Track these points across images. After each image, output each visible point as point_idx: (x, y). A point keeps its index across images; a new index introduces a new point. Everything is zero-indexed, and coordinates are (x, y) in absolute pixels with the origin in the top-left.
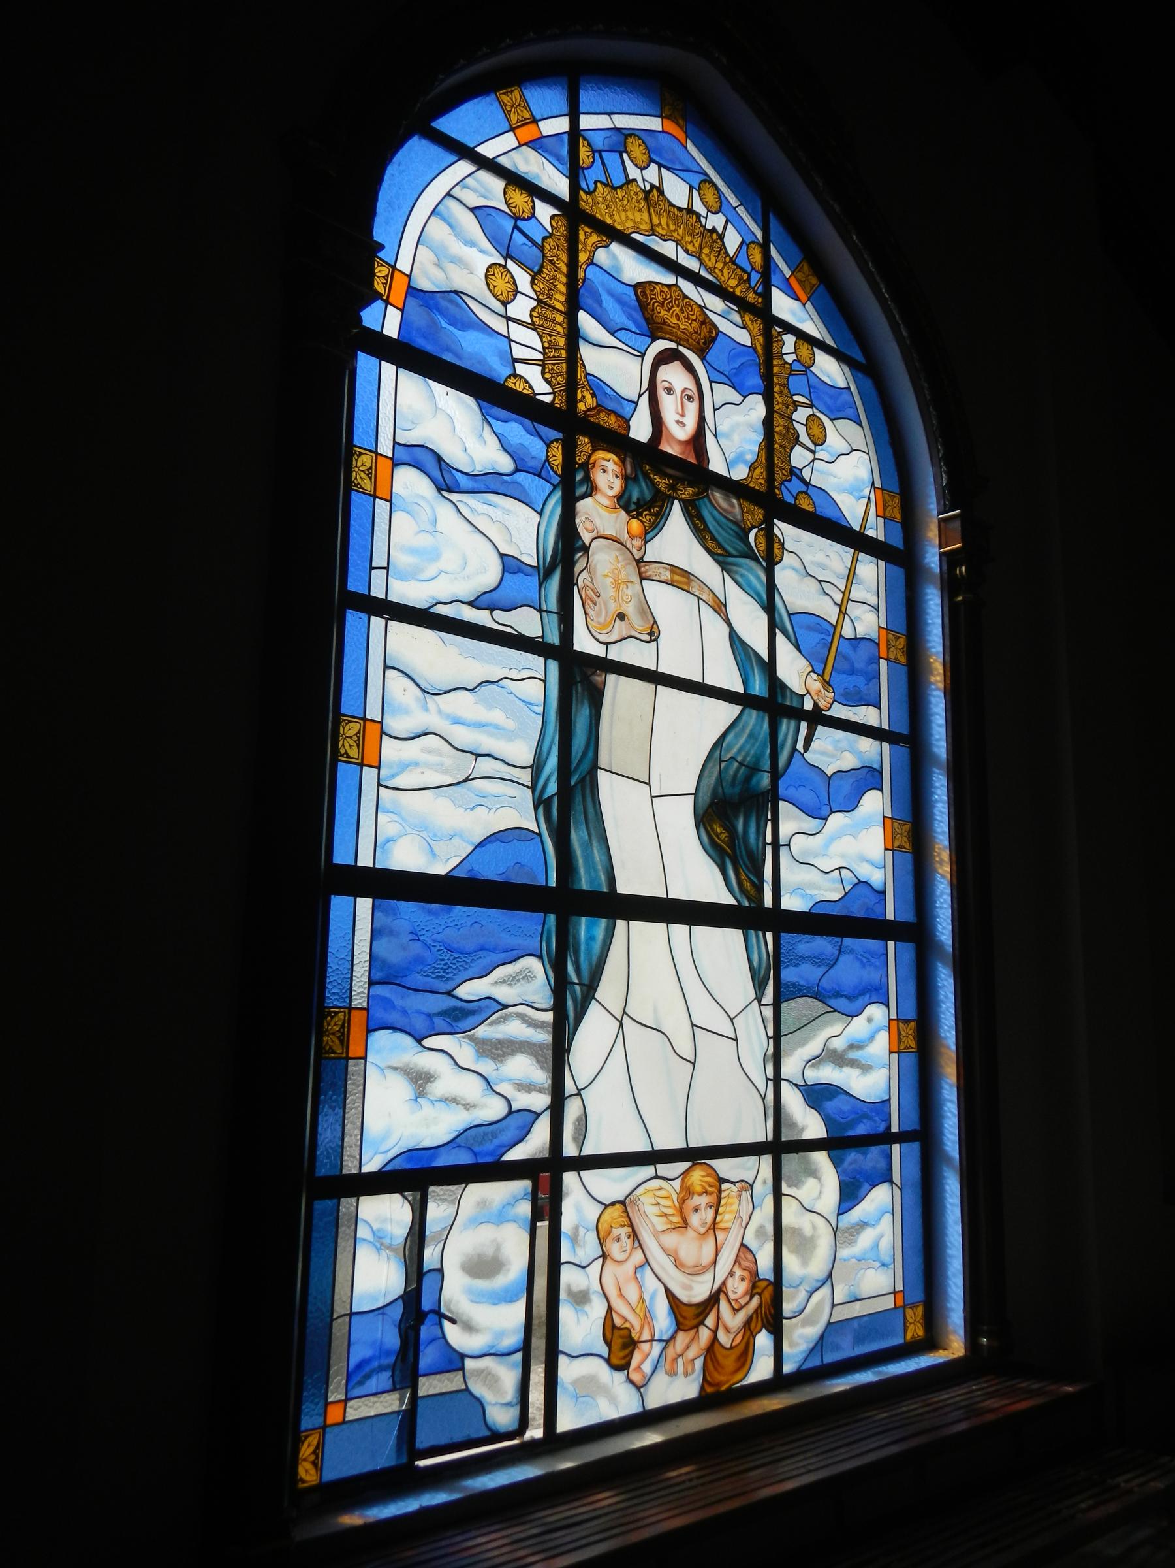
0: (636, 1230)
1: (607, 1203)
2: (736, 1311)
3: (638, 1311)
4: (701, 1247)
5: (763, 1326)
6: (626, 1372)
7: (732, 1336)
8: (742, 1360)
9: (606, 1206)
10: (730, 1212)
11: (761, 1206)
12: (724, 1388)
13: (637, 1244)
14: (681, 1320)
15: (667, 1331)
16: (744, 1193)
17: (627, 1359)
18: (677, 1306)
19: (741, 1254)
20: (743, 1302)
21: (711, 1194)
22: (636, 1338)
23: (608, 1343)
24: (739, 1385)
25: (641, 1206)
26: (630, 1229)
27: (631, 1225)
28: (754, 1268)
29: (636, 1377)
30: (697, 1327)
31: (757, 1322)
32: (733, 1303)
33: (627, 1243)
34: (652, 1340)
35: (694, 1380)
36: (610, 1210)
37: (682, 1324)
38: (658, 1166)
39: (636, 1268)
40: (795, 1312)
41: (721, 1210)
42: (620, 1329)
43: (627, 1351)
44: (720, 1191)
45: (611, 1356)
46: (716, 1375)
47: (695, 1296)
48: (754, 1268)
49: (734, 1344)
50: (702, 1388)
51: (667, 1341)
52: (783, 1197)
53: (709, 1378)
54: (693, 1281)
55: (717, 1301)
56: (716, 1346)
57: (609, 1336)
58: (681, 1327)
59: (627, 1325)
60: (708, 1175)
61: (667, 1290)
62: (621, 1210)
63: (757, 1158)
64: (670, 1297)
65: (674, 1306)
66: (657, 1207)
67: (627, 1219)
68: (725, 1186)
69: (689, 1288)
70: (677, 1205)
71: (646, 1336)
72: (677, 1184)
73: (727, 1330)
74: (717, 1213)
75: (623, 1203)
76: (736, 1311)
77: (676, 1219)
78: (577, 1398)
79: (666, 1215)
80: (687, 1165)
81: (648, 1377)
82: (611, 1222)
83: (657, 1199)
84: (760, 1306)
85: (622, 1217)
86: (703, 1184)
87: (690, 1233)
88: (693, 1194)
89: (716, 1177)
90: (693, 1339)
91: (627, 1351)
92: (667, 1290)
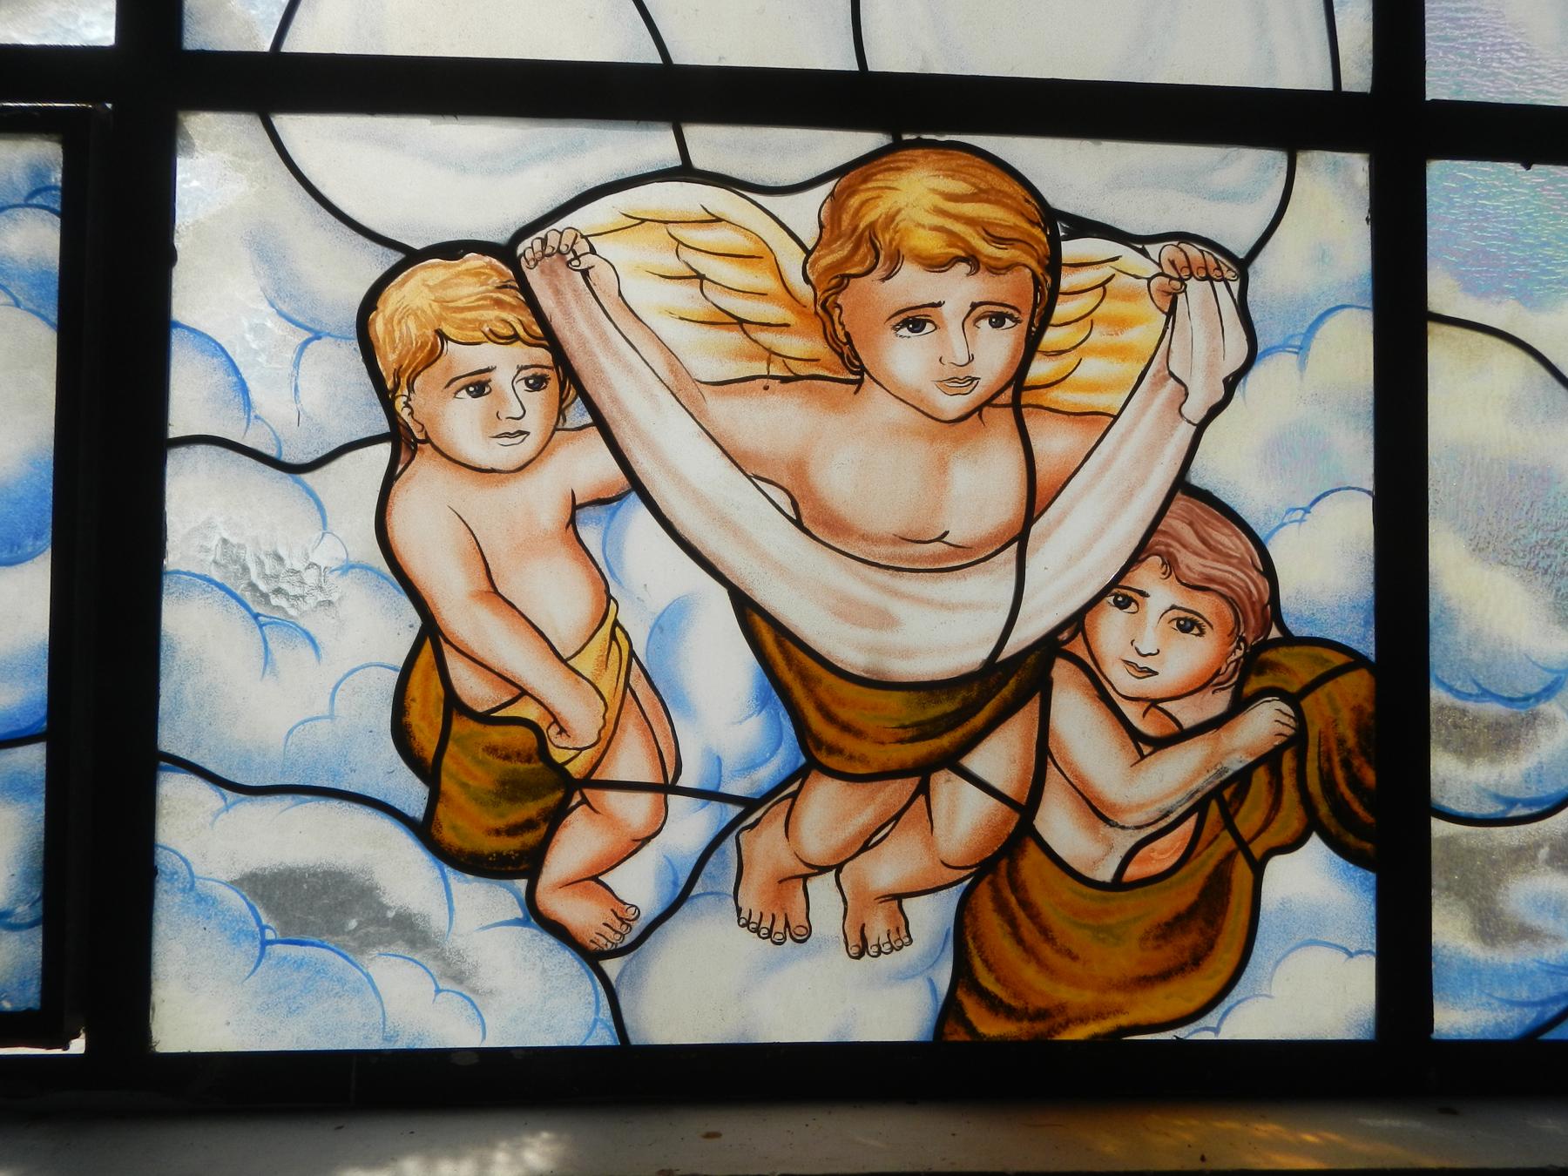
0: (579, 362)
1: (418, 246)
2: (1144, 745)
3: (585, 664)
4: (943, 466)
5: (1313, 824)
6: (521, 884)
7: (1126, 841)
8: (1189, 940)
9: (412, 257)
10: (1122, 352)
11: (1302, 350)
12: (1079, 1033)
13: (578, 415)
14: (829, 733)
15: (752, 766)
16: (1192, 284)
17: (530, 838)
18: (805, 678)
19: (1171, 522)
20: (1188, 712)
21: (996, 269)
22: (576, 768)
23: (428, 771)
24: (1183, 1033)
25: (601, 274)
26: (542, 356)
27: (551, 341)
28: (1253, 584)
29: (581, 914)
30: (922, 772)
31: (1276, 805)
32: (1132, 712)
33: (536, 409)
34: (666, 787)
35: (903, 976)
36: (433, 272)
37: (833, 750)
38: (693, 132)
39: (575, 507)
40: (1512, 803)
41: (1052, 337)
42: (486, 719)
43: (530, 809)
44: (1054, 264)
45: (441, 809)
46: (1030, 973)
47: (906, 654)
48: (1253, 584)
49: (1133, 872)
50: (950, 1011)
51: (749, 804)
52: (1433, 329)
53: (987, 981)
54: (896, 594)
55: (1041, 687)
56: (1032, 858)
57: (426, 738)
58: (823, 758)
59: (528, 711)
60: (977, 196)
61: (745, 607)
62: (496, 280)
63: (1278, 159)
64: (767, 637)
65: (788, 676)
66: (692, 289)
67: (528, 318)
68: (1072, 249)
69: (885, 620)
70: (805, 292)
71: (631, 762)
72: (804, 212)
73: (1097, 811)
74: (1032, 345)
75: (505, 252)
76: (1144, 745)
77: (801, 345)
78: (265, 943)
79: (741, 322)
80: (870, 141)
81: (638, 926)
82: (441, 318)
83: (687, 255)
84: (1297, 741)
85: (499, 303)
86: (958, 228)
87: (878, 407)
88: (896, 260)
89: (1032, 209)
90: (897, 817)
91: (530, 809)
92: (745, 607)
